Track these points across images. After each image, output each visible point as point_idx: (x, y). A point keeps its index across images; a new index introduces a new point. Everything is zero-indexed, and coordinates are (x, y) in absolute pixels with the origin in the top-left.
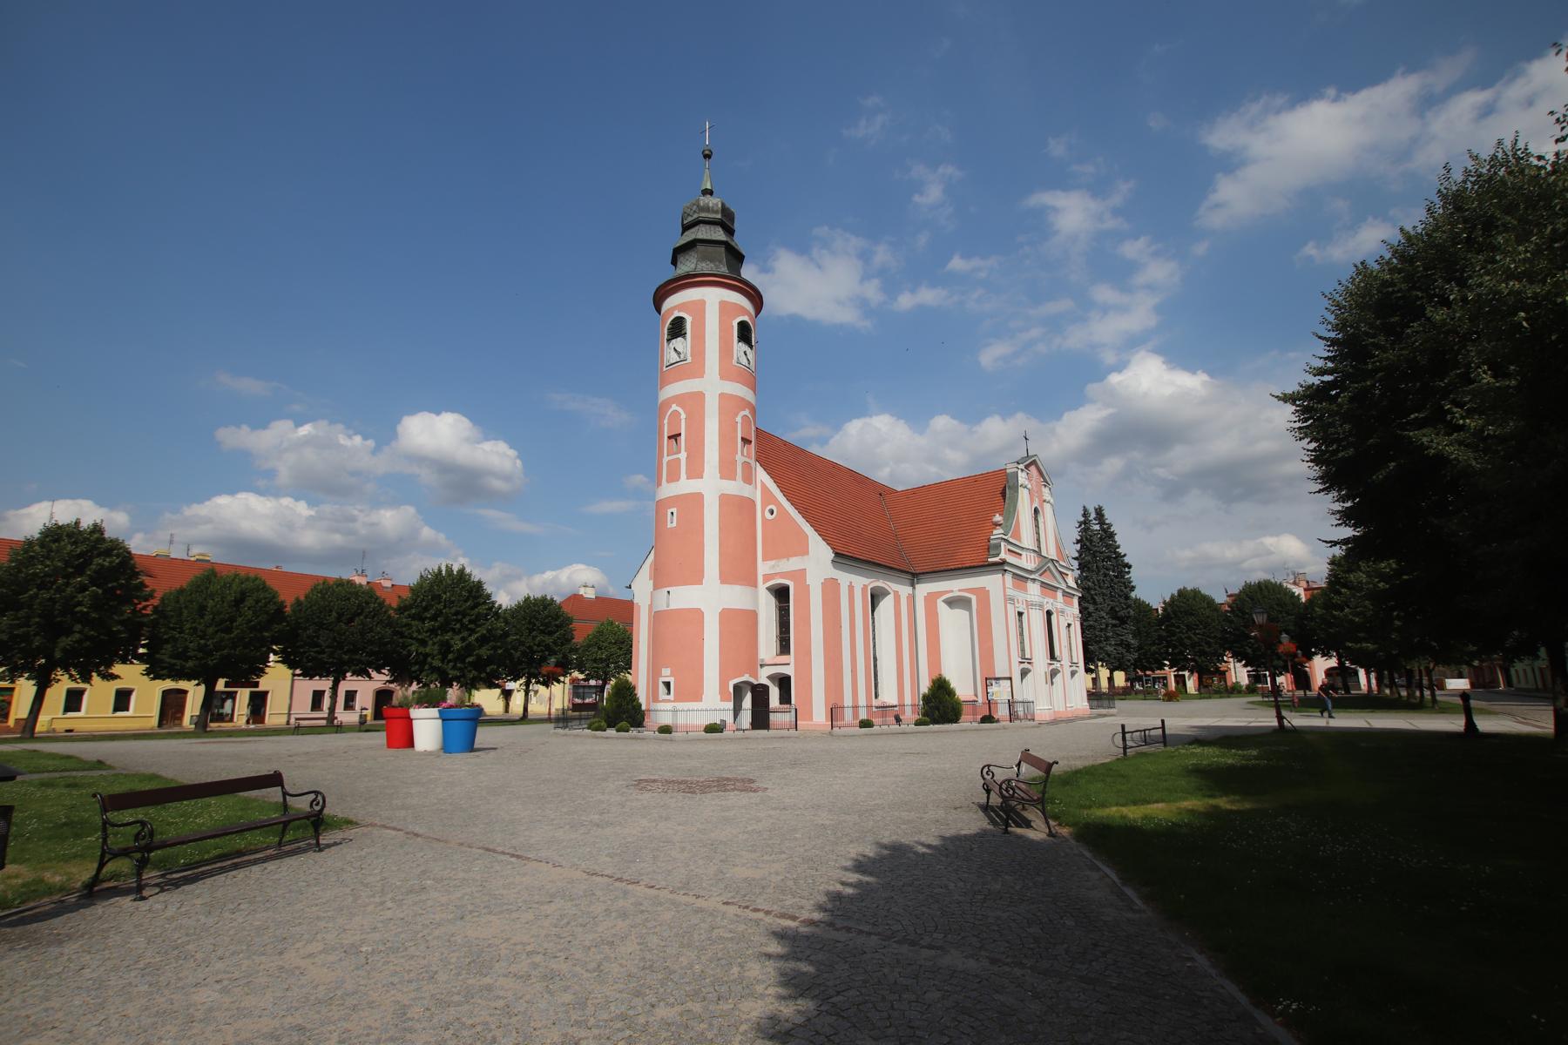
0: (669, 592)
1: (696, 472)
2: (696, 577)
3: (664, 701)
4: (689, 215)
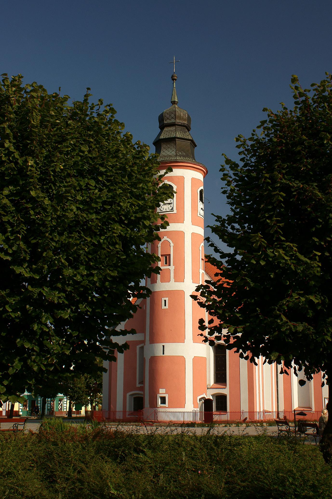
0: (163, 346)
1: (180, 278)
2: (181, 339)
3: (161, 407)
4: (168, 118)
